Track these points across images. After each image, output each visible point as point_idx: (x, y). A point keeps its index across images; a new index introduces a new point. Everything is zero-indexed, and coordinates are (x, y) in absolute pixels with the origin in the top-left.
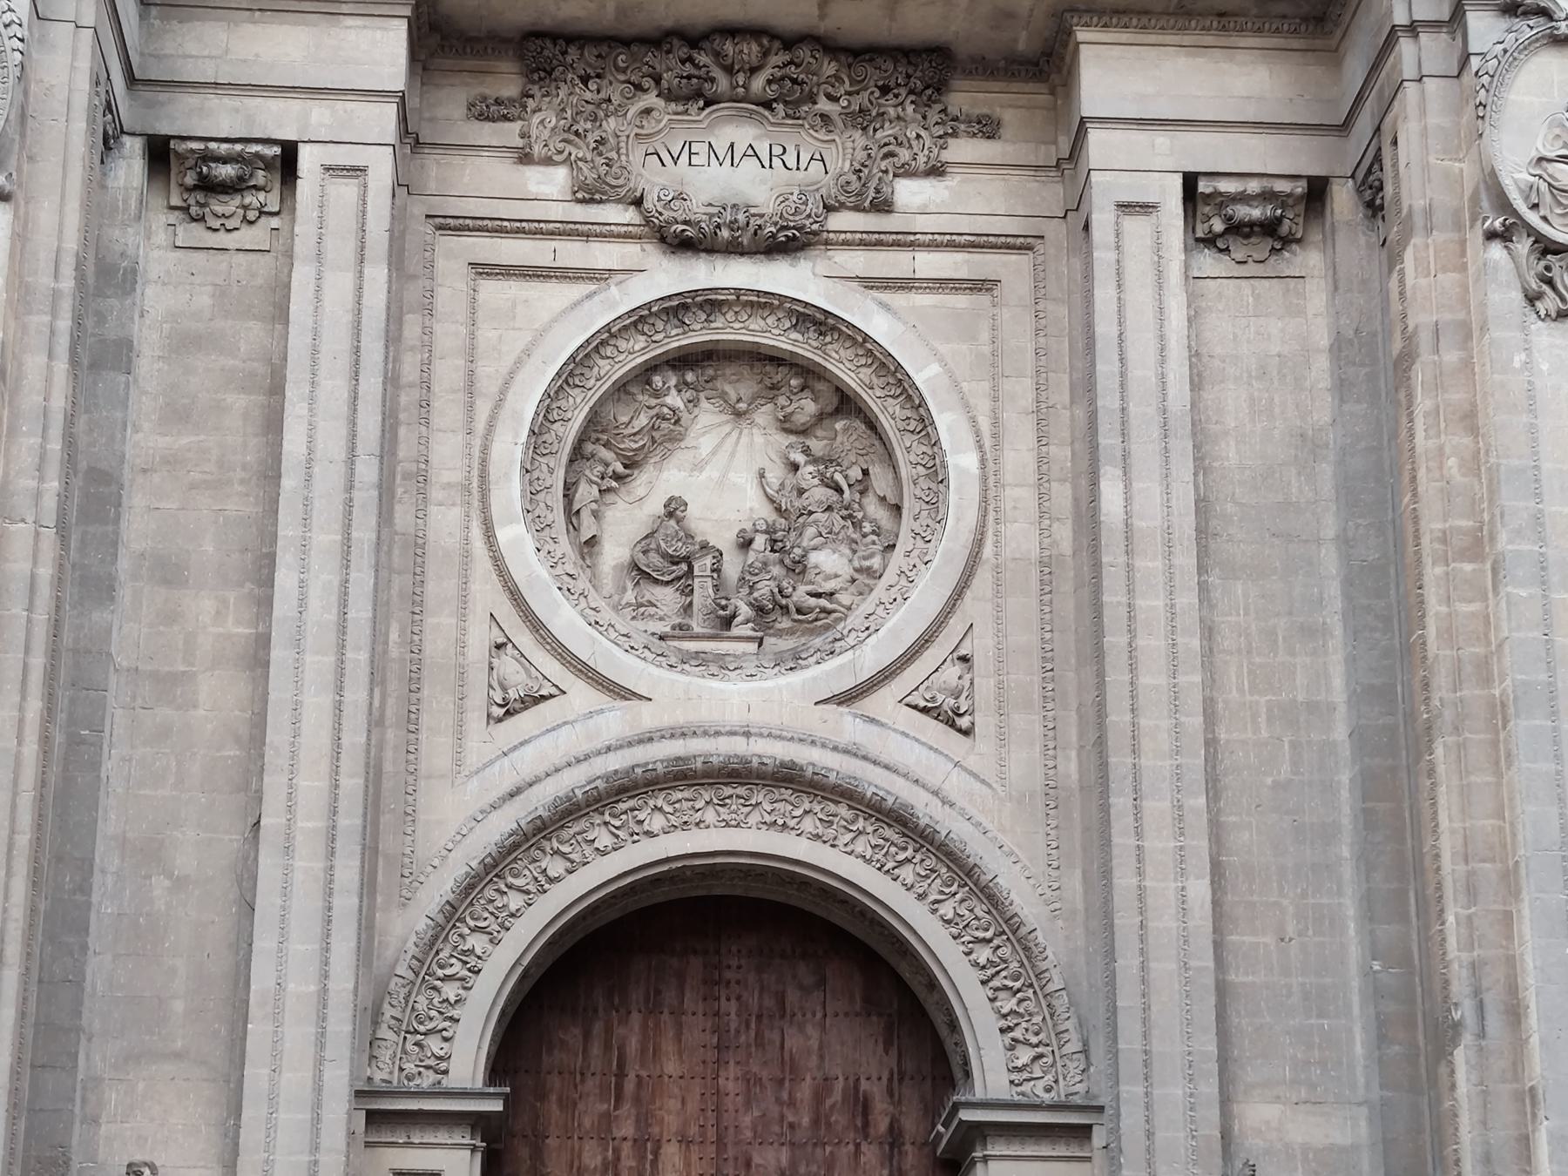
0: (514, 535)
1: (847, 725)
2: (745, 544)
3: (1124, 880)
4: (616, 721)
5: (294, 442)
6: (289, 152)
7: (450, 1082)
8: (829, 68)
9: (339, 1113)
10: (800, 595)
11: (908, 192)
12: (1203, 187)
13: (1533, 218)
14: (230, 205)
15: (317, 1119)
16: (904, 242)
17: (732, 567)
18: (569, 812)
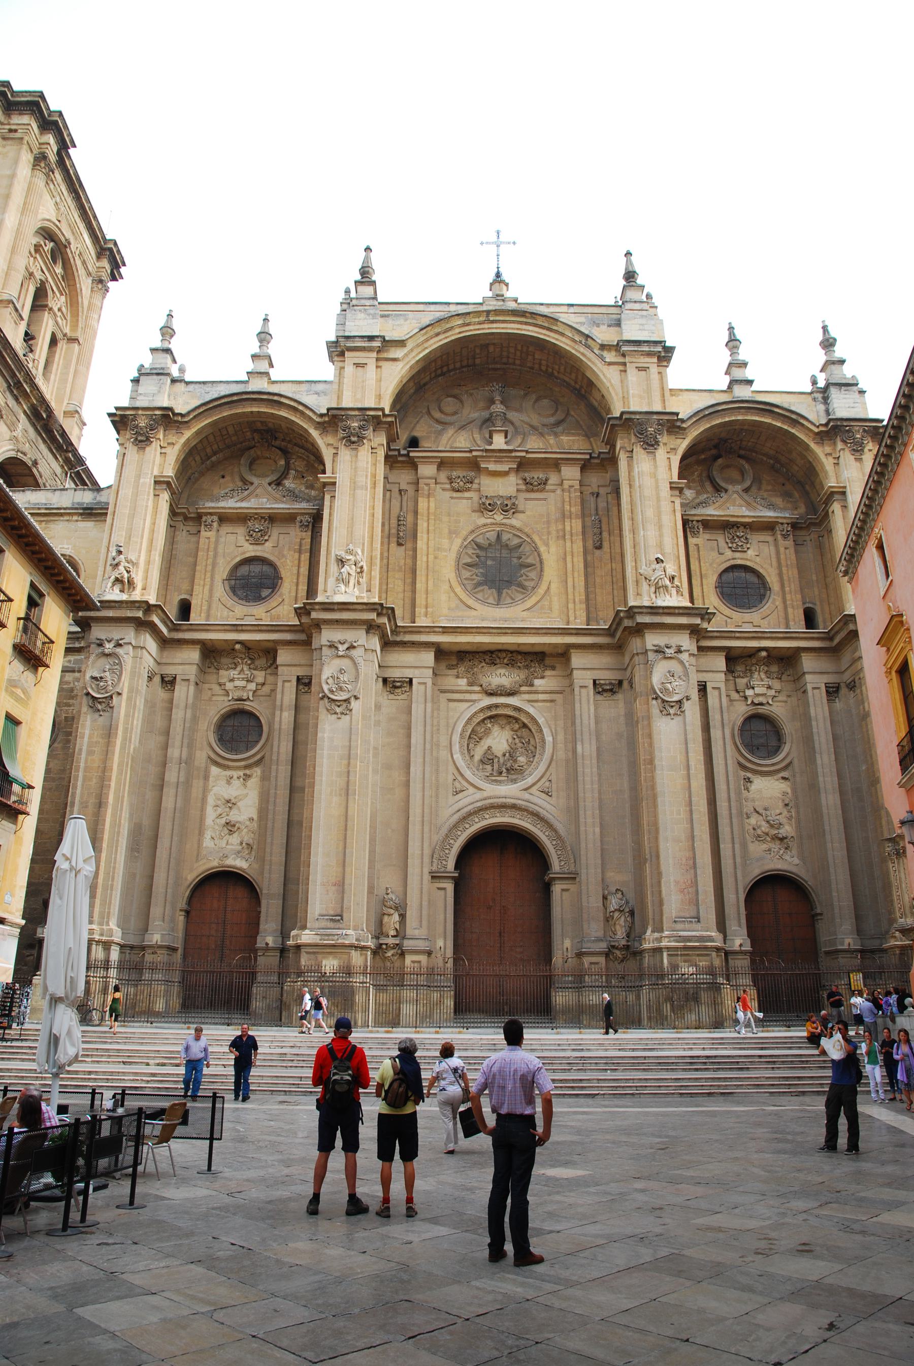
0: (457, 756)
1: (526, 796)
2: (504, 755)
4: (479, 795)
5: (413, 741)
6: (411, 680)
7: (448, 870)
8: (520, 657)
9: (427, 877)
10: (516, 766)
11: (537, 682)
12: (597, 682)
13: (661, 695)
14: (399, 690)
15: (422, 879)
16: (536, 692)
17: (502, 760)
18: (470, 814)
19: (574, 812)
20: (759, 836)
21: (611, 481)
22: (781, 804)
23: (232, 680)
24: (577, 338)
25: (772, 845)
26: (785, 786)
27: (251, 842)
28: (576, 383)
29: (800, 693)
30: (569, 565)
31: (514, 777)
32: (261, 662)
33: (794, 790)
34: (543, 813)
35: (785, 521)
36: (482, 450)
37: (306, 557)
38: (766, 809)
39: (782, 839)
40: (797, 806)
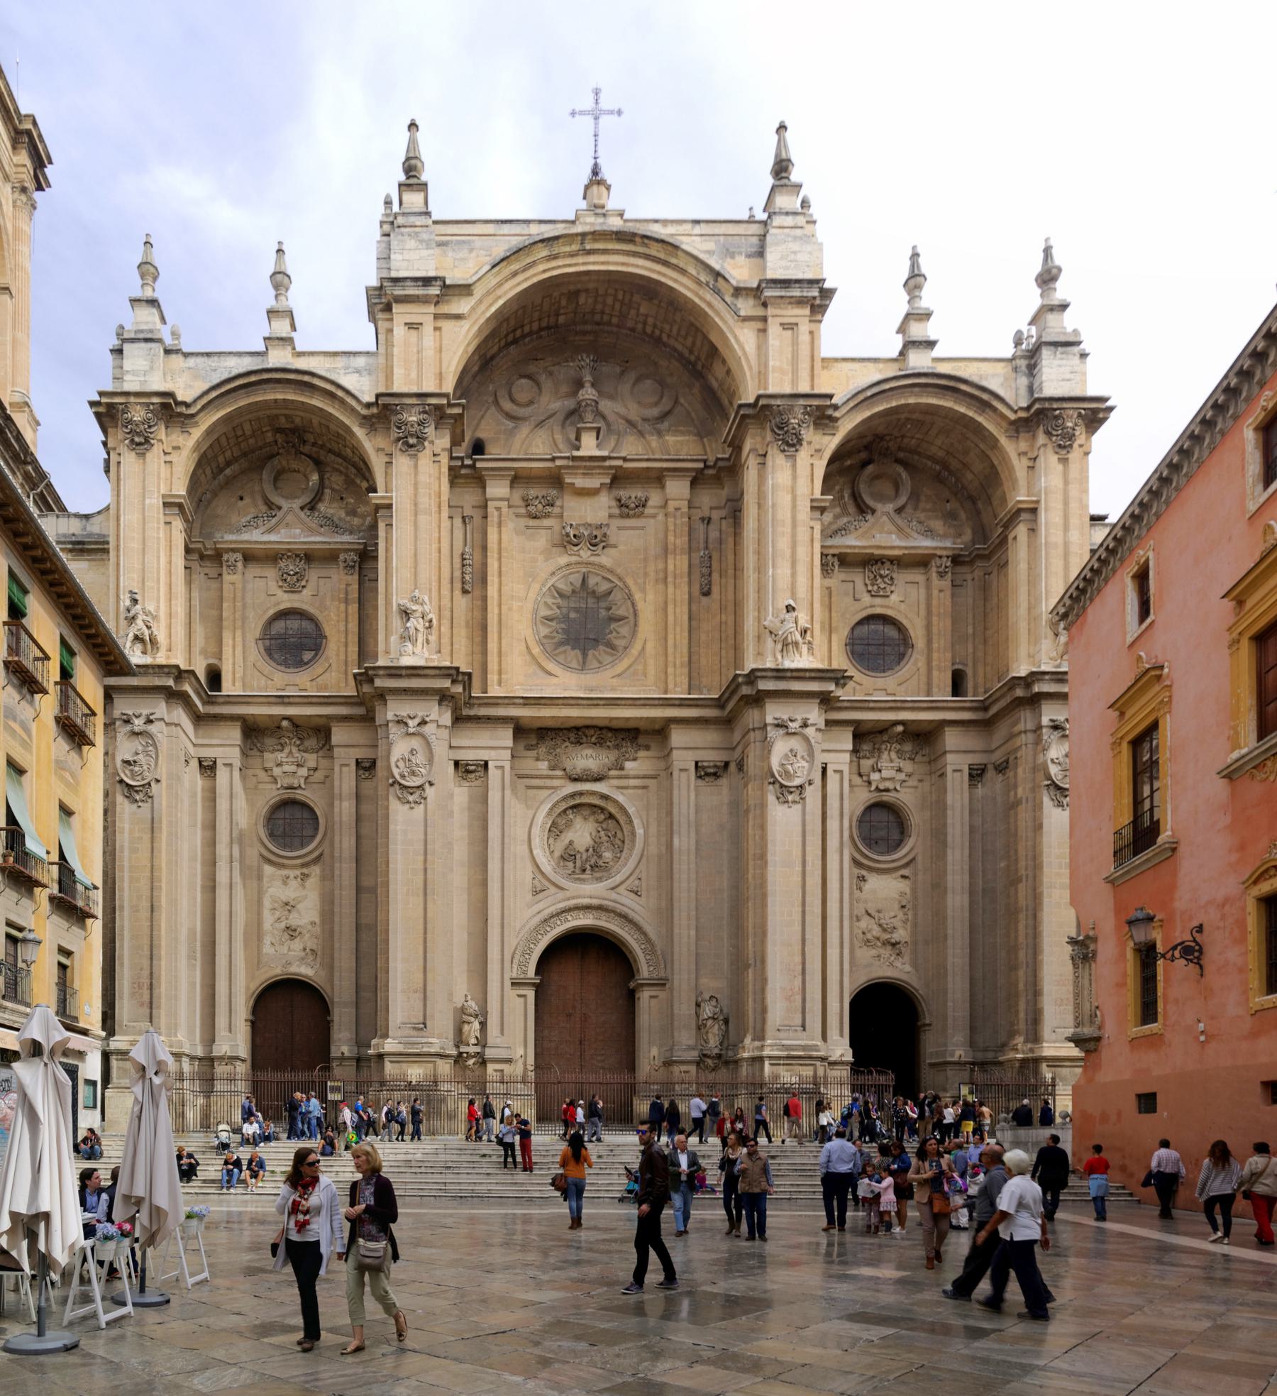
1: (613, 895)
3: (676, 931)
11: (628, 765)
16: (627, 777)
19: (667, 914)
20: (868, 941)
21: (728, 500)
22: (897, 906)
23: (279, 765)
24: (703, 278)
25: (882, 951)
26: (904, 886)
27: (315, 947)
28: (691, 352)
29: (934, 777)
30: (671, 618)
31: (598, 875)
32: (311, 742)
33: (914, 890)
34: (631, 914)
35: (944, 553)
36: (568, 458)
37: (354, 608)
38: (879, 912)
39: (894, 945)
40: (915, 907)
